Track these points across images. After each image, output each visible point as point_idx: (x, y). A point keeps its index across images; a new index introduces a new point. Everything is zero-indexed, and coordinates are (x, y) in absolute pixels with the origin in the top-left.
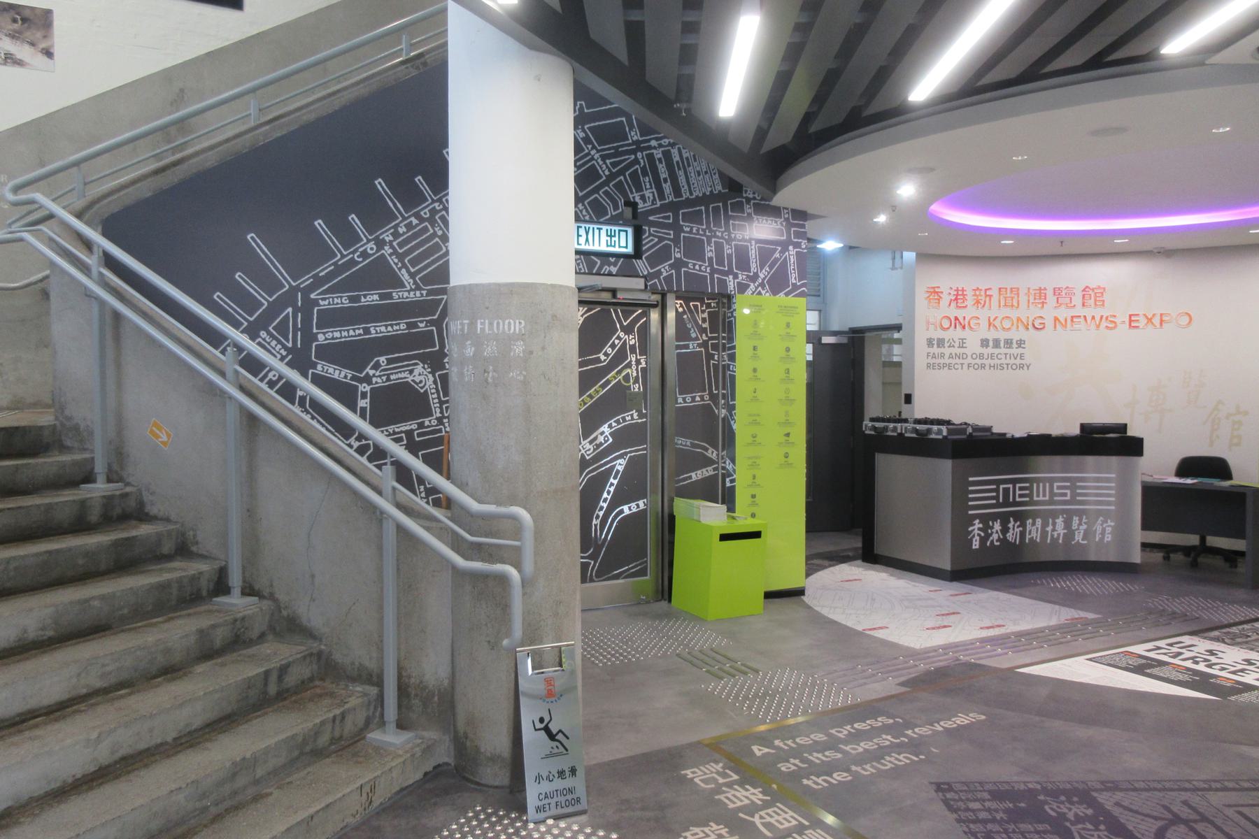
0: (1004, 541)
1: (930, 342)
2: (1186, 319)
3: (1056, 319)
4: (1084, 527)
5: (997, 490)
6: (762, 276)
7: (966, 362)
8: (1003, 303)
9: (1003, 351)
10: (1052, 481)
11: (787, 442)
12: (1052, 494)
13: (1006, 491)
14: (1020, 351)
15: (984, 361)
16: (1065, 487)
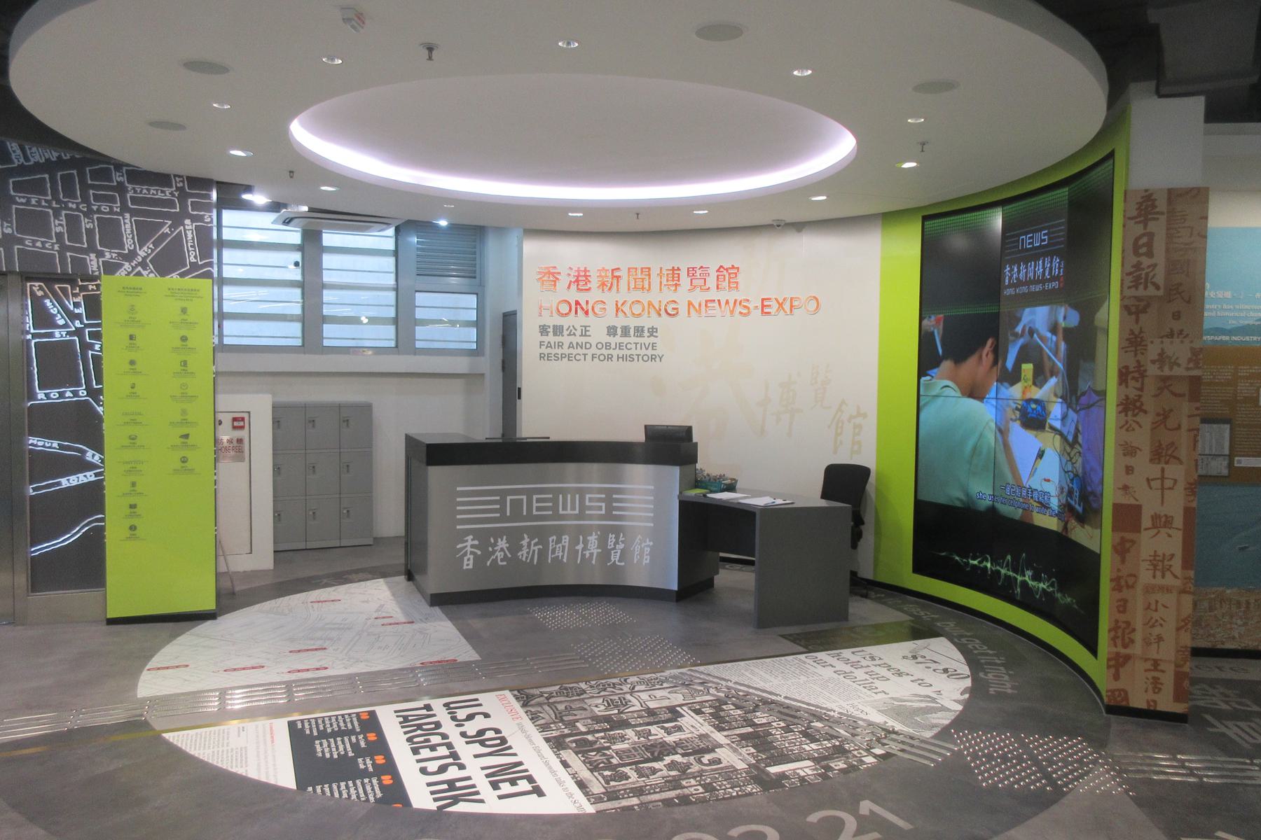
0: (513, 560)
1: (543, 330)
2: (814, 303)
3: (690, 304)
4: (621, 546)
5: (502, 503)
6: (142, 253)
7: (590, 352)
8: (632, 286)
9: (633, 339)
10: (582, 492)
11: (185, 445)
12: (583, 507)
13: (516, 505)
14: (652, 339)
15: (610, 352)
16: (600, 500)
